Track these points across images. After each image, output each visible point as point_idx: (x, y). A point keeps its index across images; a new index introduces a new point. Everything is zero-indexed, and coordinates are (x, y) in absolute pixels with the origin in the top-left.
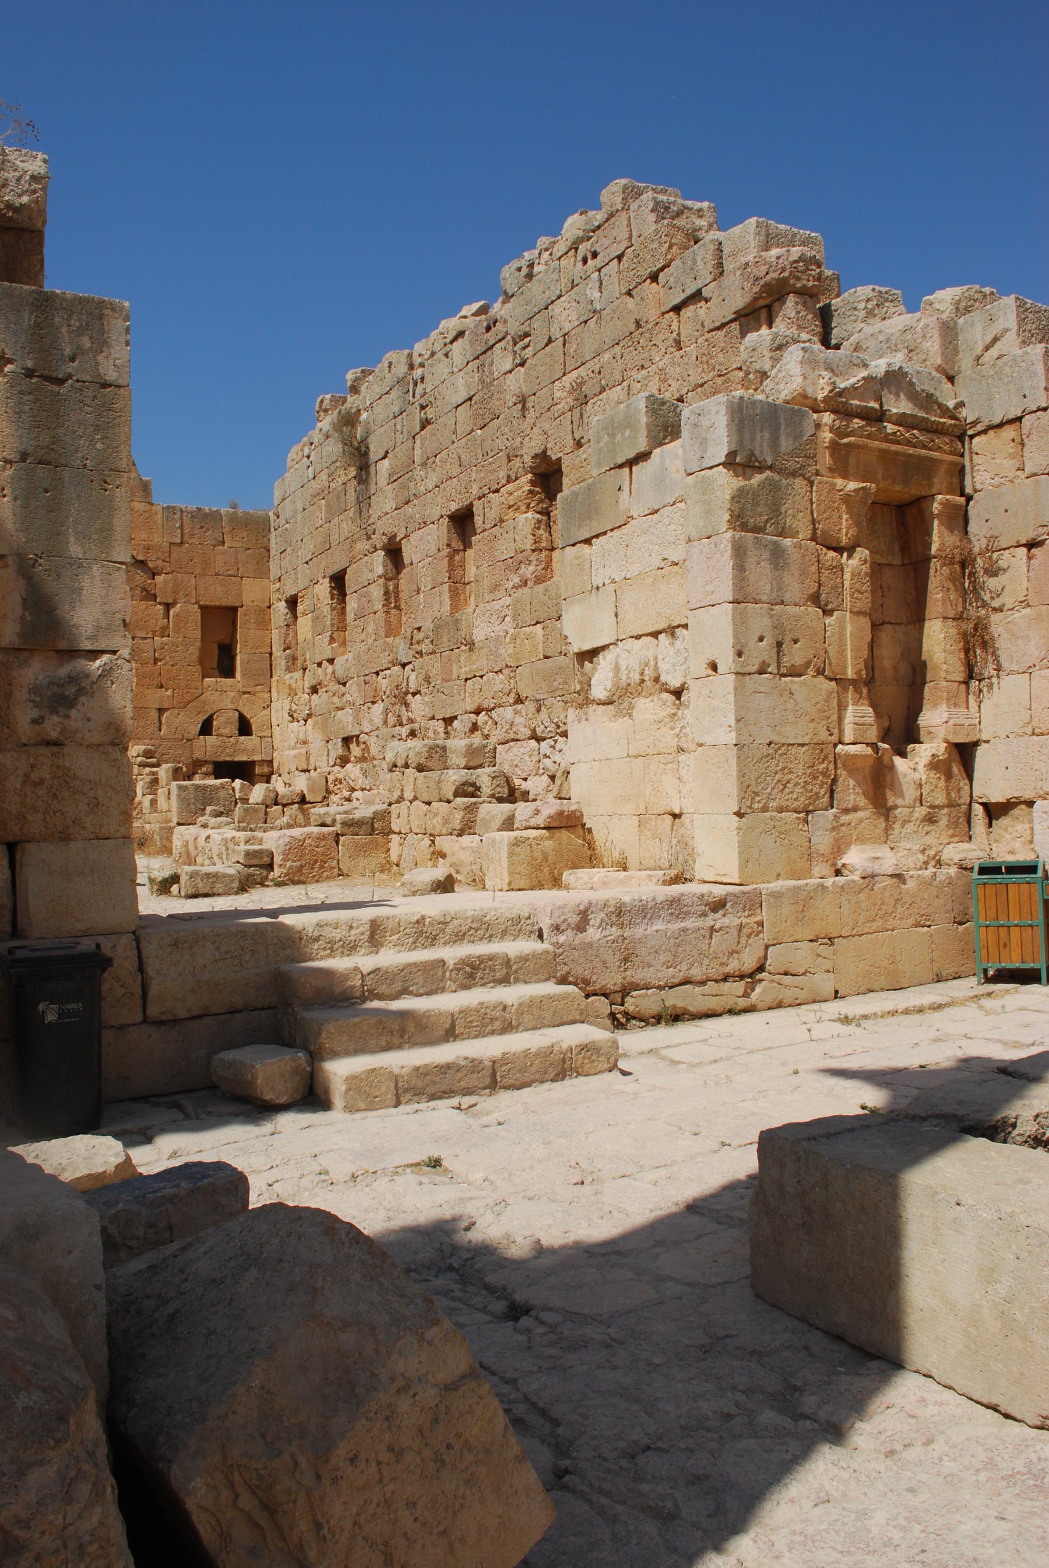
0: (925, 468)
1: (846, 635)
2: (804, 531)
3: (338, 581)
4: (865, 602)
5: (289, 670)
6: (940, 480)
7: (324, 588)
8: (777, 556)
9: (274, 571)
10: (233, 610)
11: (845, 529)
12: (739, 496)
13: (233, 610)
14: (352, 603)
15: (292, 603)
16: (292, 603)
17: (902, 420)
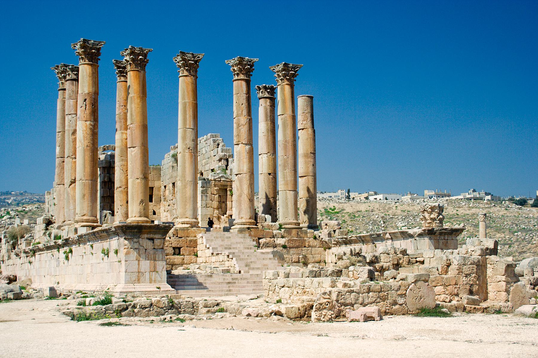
0: (227, 186)
1: (215, 204)
2: (210, 193)
3: (174, 184)
4: (217, 200)
5: (164, 201)
6: (228, 186)
7: (171, 185)
8: (206, 196)
9: (162, 180)
10: (153, 188)
11: (215, 192)
12: (202, 191)
13: (153, 188)
14: (176, 190)
15: (165, 187)
16: (165, 187)
17: (223, 181)
